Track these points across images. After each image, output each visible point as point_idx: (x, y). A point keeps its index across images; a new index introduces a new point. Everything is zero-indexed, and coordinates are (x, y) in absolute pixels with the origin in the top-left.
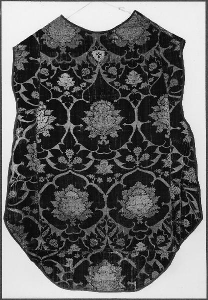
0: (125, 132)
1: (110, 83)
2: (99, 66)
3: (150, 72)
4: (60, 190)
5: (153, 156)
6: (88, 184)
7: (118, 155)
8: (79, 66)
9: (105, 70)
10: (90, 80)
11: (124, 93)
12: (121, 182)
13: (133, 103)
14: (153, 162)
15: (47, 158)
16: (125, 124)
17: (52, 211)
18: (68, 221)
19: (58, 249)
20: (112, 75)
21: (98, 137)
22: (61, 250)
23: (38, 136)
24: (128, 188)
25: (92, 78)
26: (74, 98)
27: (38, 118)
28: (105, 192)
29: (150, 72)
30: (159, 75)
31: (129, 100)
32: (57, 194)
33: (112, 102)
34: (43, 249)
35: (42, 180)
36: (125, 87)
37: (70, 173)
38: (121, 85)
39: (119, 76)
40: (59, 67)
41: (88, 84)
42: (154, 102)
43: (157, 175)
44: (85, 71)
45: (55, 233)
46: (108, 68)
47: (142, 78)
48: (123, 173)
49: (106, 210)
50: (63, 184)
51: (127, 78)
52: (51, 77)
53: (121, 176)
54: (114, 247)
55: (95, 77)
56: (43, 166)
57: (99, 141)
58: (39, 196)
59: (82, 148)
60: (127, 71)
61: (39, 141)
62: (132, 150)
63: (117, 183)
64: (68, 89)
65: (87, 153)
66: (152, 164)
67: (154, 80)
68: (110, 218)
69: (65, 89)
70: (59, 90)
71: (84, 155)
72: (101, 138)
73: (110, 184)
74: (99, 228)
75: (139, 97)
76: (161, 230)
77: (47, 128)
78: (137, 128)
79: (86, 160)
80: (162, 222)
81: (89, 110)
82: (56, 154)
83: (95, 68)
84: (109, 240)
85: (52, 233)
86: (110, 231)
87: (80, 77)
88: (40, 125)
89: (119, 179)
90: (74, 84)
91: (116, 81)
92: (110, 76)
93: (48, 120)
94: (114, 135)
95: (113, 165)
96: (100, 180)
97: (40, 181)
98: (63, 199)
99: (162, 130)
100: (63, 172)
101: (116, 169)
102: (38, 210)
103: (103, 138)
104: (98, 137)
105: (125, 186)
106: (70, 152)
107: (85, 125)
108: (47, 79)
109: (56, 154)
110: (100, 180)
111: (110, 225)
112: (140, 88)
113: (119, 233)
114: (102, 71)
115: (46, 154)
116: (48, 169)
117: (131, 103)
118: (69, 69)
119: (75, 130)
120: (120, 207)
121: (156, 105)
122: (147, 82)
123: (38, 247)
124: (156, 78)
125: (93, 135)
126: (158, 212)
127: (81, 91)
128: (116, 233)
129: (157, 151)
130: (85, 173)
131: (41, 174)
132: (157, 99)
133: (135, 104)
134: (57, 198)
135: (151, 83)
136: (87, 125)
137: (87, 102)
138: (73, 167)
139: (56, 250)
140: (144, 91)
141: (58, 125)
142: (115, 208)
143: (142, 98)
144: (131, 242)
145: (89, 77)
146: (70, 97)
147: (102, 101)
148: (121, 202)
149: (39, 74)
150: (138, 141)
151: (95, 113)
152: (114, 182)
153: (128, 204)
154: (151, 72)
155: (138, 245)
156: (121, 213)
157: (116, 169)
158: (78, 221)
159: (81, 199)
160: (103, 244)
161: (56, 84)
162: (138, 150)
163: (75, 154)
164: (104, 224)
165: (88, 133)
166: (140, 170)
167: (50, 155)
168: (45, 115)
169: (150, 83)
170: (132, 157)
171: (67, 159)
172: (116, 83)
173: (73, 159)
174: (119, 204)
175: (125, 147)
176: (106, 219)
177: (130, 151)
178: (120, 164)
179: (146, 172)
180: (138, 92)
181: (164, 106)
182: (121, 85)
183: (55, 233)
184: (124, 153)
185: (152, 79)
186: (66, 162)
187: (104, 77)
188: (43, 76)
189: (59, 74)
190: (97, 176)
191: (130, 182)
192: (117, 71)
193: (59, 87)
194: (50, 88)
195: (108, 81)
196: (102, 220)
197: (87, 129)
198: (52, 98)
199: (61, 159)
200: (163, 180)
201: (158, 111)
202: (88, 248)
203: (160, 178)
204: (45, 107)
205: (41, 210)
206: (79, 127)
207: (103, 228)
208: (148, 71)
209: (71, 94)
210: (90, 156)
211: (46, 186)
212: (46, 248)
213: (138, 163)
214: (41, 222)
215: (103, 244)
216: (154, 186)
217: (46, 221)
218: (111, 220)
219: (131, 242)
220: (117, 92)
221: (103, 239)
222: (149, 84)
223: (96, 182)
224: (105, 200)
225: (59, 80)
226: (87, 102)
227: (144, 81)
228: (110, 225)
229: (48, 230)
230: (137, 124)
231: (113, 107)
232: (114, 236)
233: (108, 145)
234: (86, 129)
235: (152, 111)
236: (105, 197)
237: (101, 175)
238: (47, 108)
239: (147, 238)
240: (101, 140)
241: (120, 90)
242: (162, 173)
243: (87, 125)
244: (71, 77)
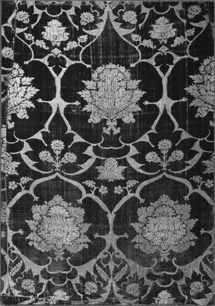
0: (146, 115)
1: (124, 36)
2: (108, 10)
3: (189, 20)
4: (41, 203)
5: (190, 154)
6: (85, 195)
7: (133, 151)
8: (77, 9)
9: (117, 15)
11: (147, 52)
12: (137, 195)
13: (161, 69)
14: (188, 165)
15: (22, 152)
16: (146, 103)
17: (27, 235)
18: (52, 253)
19: (35, 295)
20: (128, 23)
21: (104, 121)
22: (40, 296)
23: (9, 118)
24: (147, 204)
25: (96, 27)
26: (67, 59)
27: (11, 90)
28: (111, 210)
29: (189, 20)
30: (203, 24)
32: (37, 210)
33: (127, 67)
34: (12, 294)
35: (13, 185)
36: (147, 43)
37: (57, 177)
38: (142, 40)
39: (140, 26)
40: (46, 11)
41: (90, 38)
42: (194, 68)
43: (195, 186)
44: (87, 17)
45: (30, 271)
46: (122, 13)
47: (176, 30)
48: (141, 181)
49: (111, 239)
50: (44, 194)
51: (152, 29)
52: (33, 26)
53: (137, 185)
54: (122, 296)
55: (101, 26)
56: (16, 164)
57: (104, 128)
58: (8, 211)
59: (78, 139)
60: (153, 18)
61: (11, 125)
62: (156, 144)
63: (130, 195)
64: (58, 45)
65: (84, 146)
66: (187, 169)
67: (196, 34)
68: (116, 250)
69: (53, 44)
70: (44, 47)
71: (79, 149)
72: (107, 124)
73: (119, 197)
74: (100, 265)
75: (170, 59)
76: (198, 272)
77: (23, 105)
78: (165, 110)
79: (83, 158)
80: (200, 259)
81: (90, 79)
82: (37, 146)
83: (102, 12)
84: (114, 285)
85: (26, 270)
86: (116, 271)
87: (77, 27)
88: (14, 100)
89: (134, 190)
90: (67, 38)
91: (134, 33)
92: (125, 25)
93: (26, 92)
94: (129, 119)
95: (125, 167)
96: (103, 190)
97: (10, 187)
98: (44, 217)
99: (205, 114)
100: (47, 175)
101: (130, 173)
102: (6, 234)
103: (112, 125)
104: (104, 121)
105: (142, 201)
106: (57, 145)
107: (84, 103)
108: (26, 28)
109: (37, 146)
110: (103, 190)
111: (117, 261)
112: (172, 46)
113: (131, 274)
114: (113, 17)
115: (20, 146)
116: (23, 170)
117: (158, 68)
118: (61, 13)
119: (67, 109)
120: (133, 233)
121: (198, 72)
122: (184, 35)
123: (4, 292)
124: (198, 30)
125: (94, 119)
126: (193, 244)
127: (79, 49)
128: (126, 275)
129: (196, 147)
130: (81, 178)
131: (12, 178)
132: (198, 64)
133: (164, 70)
134: (36, 216)
135: (190, 38)
136: (87, 103)
137: (88, 66)
138: (62, 168)
139: (31, 297)
140: (180, 50)
141: (40, 101)
142: (126, 235)
143: (175, 62)
144: (149, 289)
145: (92, 25)
146: (62, 58)
147: (111, 65)
148: (136, 226)
149: (14, 20)
150: (165, 130)
151: (100, 84)
152: (125, 193)
153: (147, 230)
154: (191, 20)
155: (160, 295)
156: (135, 243)
157: (130, 173)
158: (67, 254)
159: (72, 219)
160: (105, 291)
161: (38, 36)
162: (165, 145)
163: (66, 147)
164: (107, 260)
165: (87, 115)
166: (167, 176)
167: (27, 148)
168: (21, 85)
169: (188, 37)
170: (156, 155)
171: (53, 155)
172: (135, 37)
173: (62, 155)
174: (132, 228)
175: (145, 138)
176: (111, 253)
177: (153, 146)
178: (136, 166)
179: (177, 179)
180: (169, 52)
181: (209, 74)
182: (142, 40)
183: (30, 271)
184: (144, 149)
185: (191, 32)
186: (51, 160)
187: (116, 26)
188: (20, 24)
189: (45, 20)
190: (99, 183)
191: (150, 195)
192: (137, 18)
193: (45, 41)
194: (29, 42)
195: (122, 32)
196: (105, 253)
197: (87, 108)
198: (32, 59)
199: (44, 155)
200: (203, 194)
201: (200, 83)
202: (82, 296)
203: (199, 191)
204: (22, 72)
205: (11, 233)
206: (75, 105)
207: (105, 266)
208: (186, 18)
209: (63, 52)
210: (89, 151)
211: (19, 195)
212: (16, 293)
213: (164, 165)
214: (10, 252)
215: (105, 291)
216: (188, 203)
217: (17, 251)
218: (118, 254)
219: (149, 289)
220: (135, 52)
221: (106, 284)
222: (186, 39)
223: (97, 193)
224: (111, 221)
225: (44, 30)
226: (88, 66)
227: (180, 33)
228: (117, 261)
229: (19, 265)
230: (165, 103)
231: (128, 75)
232: (124, 279)
233: (118, 135)
234: (84, 109)
235: (191, 82)
236: (111, 217)
237: (105, 183)
238: (26, 75)
239: (175, 284)
240: (107, 127)
241: (141, 47)
242: (202, 183)
243: (87, 103)
244: (63, 25)
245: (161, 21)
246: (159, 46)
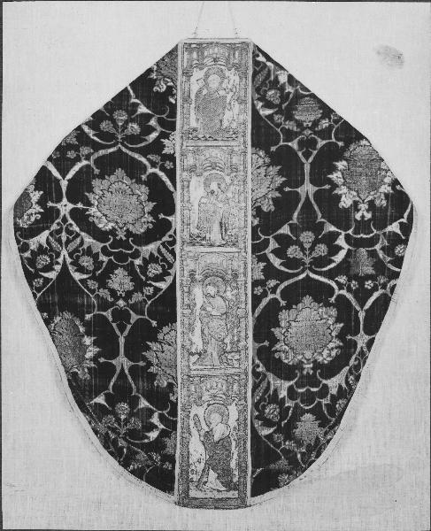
10: (50, 273)
16: (102, 360)
31: (110, 319)
38: (99, 288)
55: (58, 268)
83: (58, 255)
92: (81, 269)
114: (69, 260)
143: (132, 321)
145: (49, 268)
182: (99, 288)
195: (77, 276)
245: (119, 271)
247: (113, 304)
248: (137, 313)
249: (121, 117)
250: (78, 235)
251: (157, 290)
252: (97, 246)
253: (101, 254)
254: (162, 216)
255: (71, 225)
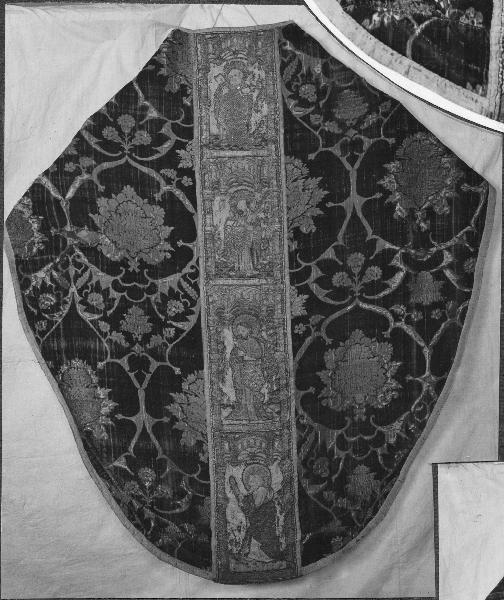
38: (111, 331)
92: (91, 309)
114: (78, 298)
143: (152, 370)
182: (111, 331)
187: (80, 308)
195: (87, 317)
230: (142, 419)
246: (133, 344)
247: (129, 350)
248: (157, 360)
249: (127, 122)
250: (86, 268)
251: (179, 331)
252: (106, 280)
253: (112, 291)
254: (180, 243)
255: (79, 256)
